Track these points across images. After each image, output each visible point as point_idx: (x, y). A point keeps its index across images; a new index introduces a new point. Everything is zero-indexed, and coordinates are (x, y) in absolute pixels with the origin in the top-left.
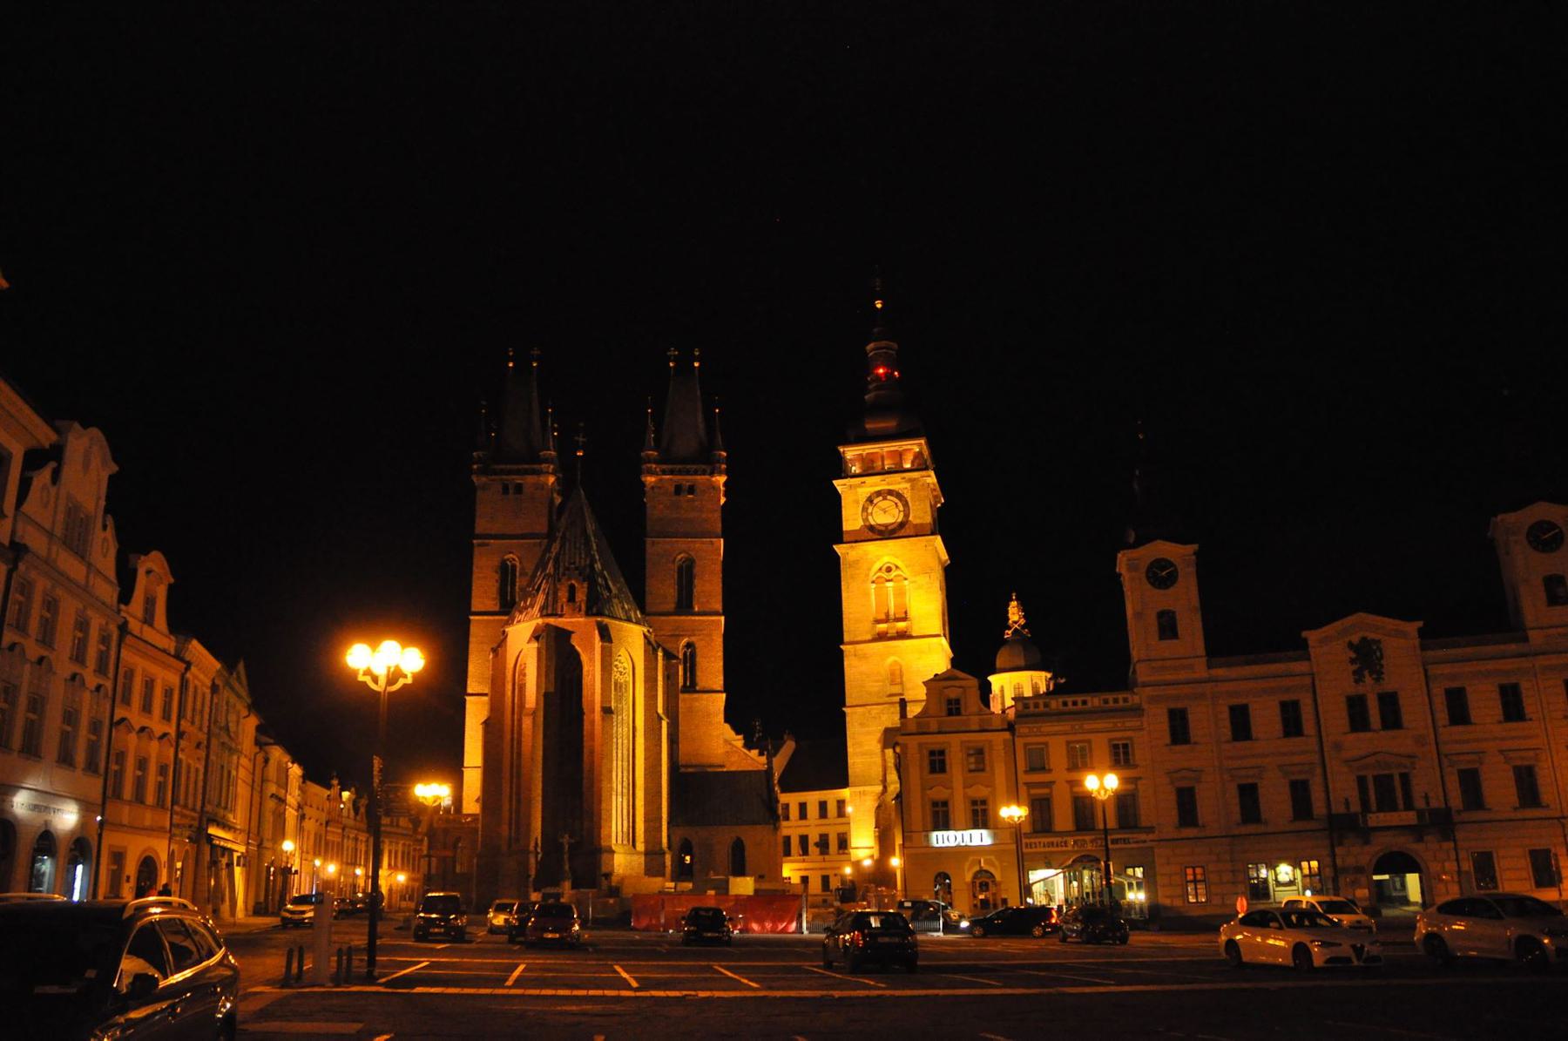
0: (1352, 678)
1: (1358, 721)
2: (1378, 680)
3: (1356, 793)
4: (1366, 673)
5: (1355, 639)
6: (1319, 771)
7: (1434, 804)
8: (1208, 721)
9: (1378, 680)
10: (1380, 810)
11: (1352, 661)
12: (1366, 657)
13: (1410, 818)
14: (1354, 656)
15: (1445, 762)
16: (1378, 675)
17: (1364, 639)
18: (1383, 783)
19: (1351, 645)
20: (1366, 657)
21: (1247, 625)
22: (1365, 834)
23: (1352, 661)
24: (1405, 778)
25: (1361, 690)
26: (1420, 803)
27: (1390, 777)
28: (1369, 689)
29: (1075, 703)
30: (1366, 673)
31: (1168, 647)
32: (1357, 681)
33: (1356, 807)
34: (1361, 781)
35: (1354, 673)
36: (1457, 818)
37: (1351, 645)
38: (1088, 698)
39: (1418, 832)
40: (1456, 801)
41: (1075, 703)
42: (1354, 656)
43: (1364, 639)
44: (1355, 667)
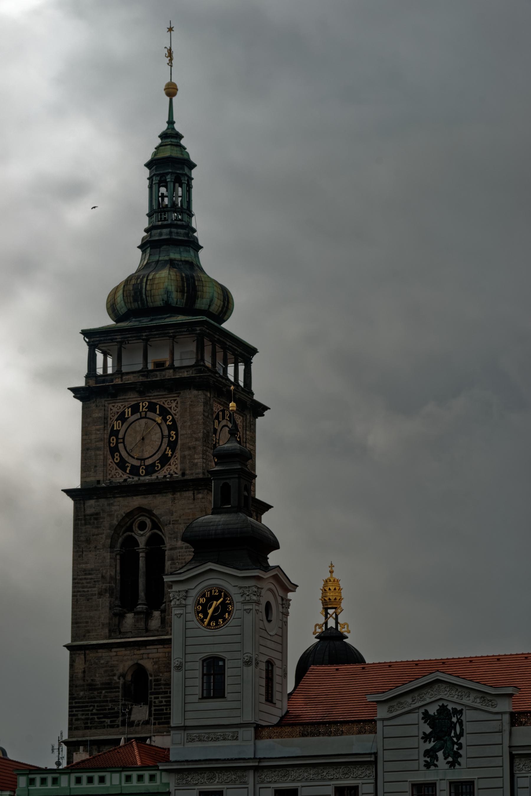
0: (422, 759)
2: (452, 765)
4: (440, 754)
5: (433, 710)
9: (452, 765)
11: (426, 737)
14: (428, 730)
17: (443, 709)
19: (426, 716)
23: (426, 737)
25: (429, 776)
29: (90, 780)
30: (440, 754)
31: (214, 711)
32: (428, 765)
35: (427, 753)
37: (426, 716)
38: (107, 775)
42: (428, 730)
43: (443, 709)
44: (429, 745)
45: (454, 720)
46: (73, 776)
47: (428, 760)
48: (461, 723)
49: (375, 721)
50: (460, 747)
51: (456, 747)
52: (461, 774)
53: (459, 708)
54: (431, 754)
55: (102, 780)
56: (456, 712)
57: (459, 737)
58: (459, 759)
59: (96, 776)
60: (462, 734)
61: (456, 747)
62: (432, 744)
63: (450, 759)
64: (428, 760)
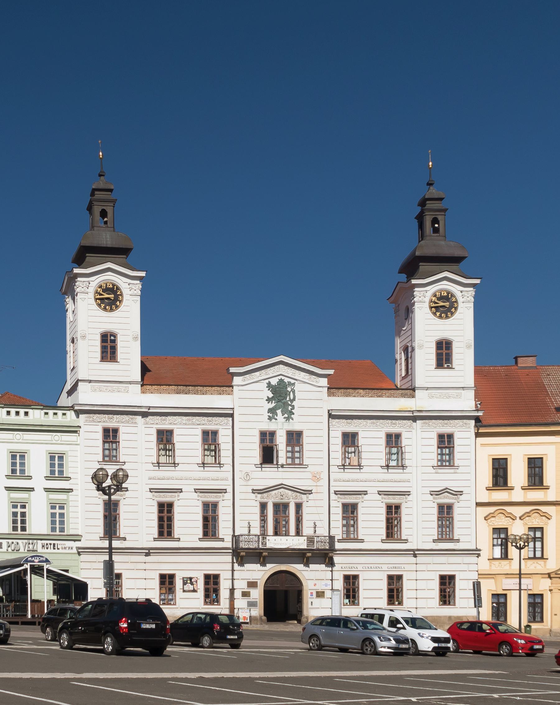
0: (266, 415)
1: (268, 455)
2: (288, 419)
3: (257, 517)
6: (229, 496)
7: (319, 532)
8: (137, 441)
9: (288, 419)
10: (276, 533)
11: (269, 400)
12: (281, 396)
13: (300, 543)
14: (271, 395)
15: (333, 496)
16: (289, 415)
18: (281, 508)
20: (281, 396)
21: (181, 357)
22: (260, 556)
23: (269, 400)
24: (299, 506)
26: (307, 530)
27: (286, 506)
28: (280, 427)
29: (17, 413)
30: (279, 412)
32: (270, 419)
33: (256, 530)
34: (263, 506)
35: (270, 410)
36: (338, 546)
38: (30, 411)
39: (302, 557)
40: (338, 532)
41: (17, 413)
42: (271, 395)
44: (272, 405)
45: (289, 389)
46: (5, 410)
47: (271, 415)
48: (294, 392)
49: (232, 387)
50: (293, 407)
51: (290, 408)
52: (295, 426)
53: (293, 381)
54: (272, 411)
55: (26, 414)
56: (290, 384)
57: (292, 401)
58: (292, 416)
59: (22, 411)
60: (294, 399)
61: (290, 408)
62: (273, 405)
63: (286, 415)
64: (271, 415)
